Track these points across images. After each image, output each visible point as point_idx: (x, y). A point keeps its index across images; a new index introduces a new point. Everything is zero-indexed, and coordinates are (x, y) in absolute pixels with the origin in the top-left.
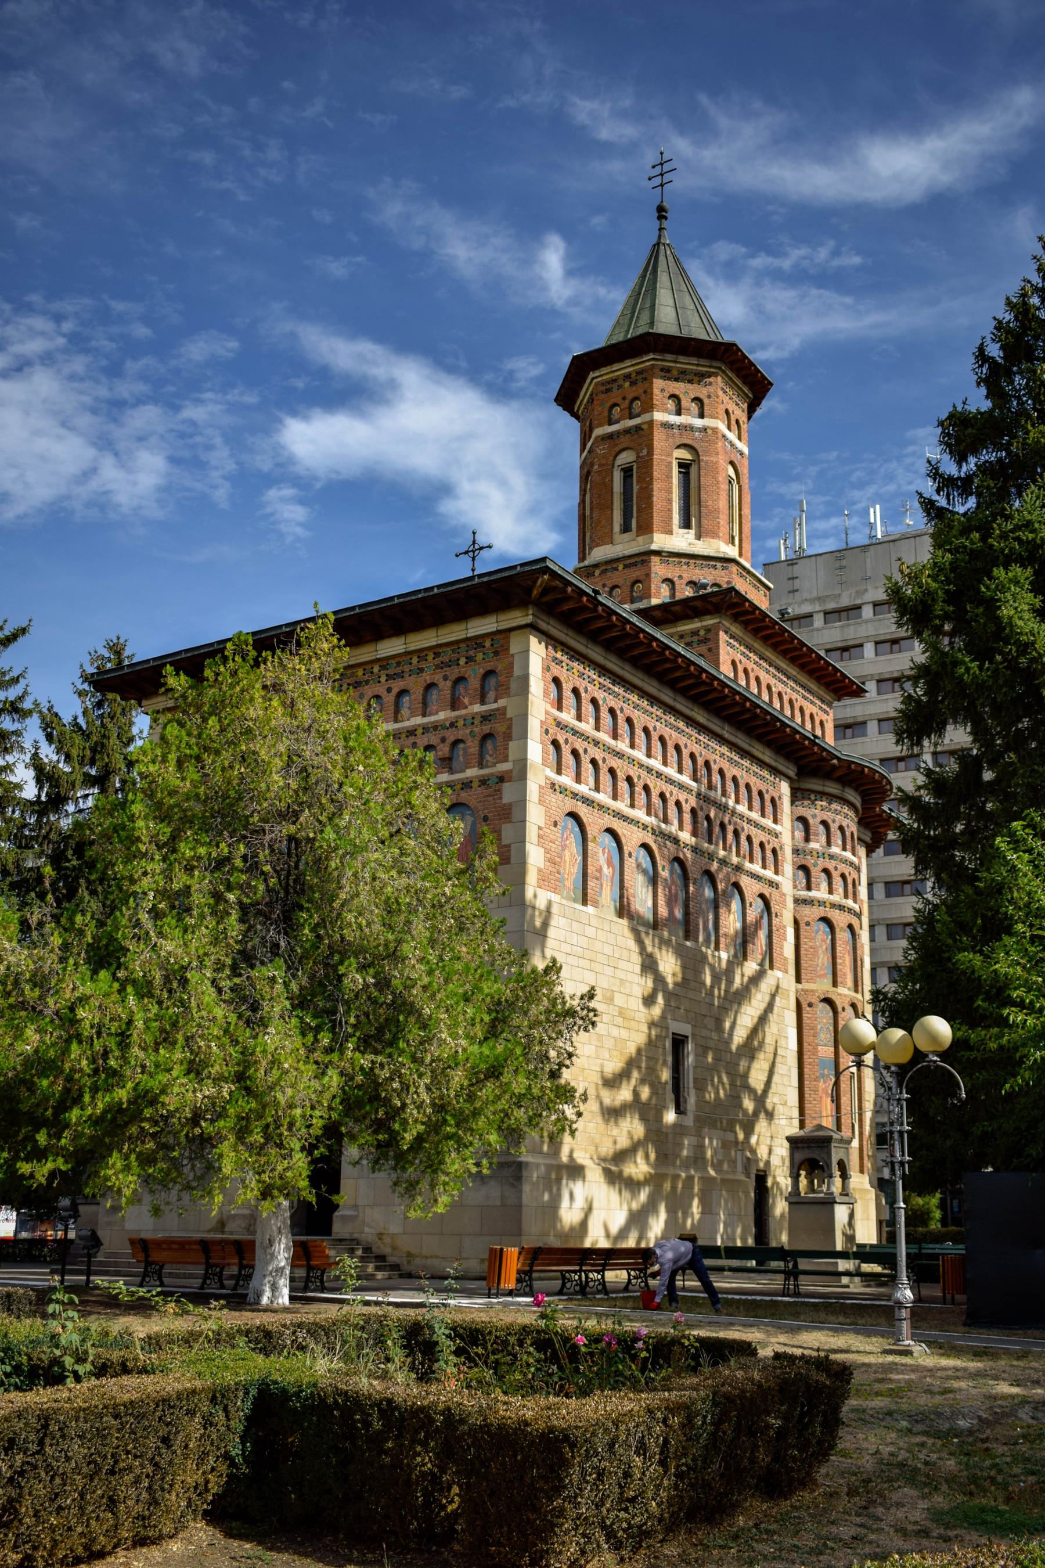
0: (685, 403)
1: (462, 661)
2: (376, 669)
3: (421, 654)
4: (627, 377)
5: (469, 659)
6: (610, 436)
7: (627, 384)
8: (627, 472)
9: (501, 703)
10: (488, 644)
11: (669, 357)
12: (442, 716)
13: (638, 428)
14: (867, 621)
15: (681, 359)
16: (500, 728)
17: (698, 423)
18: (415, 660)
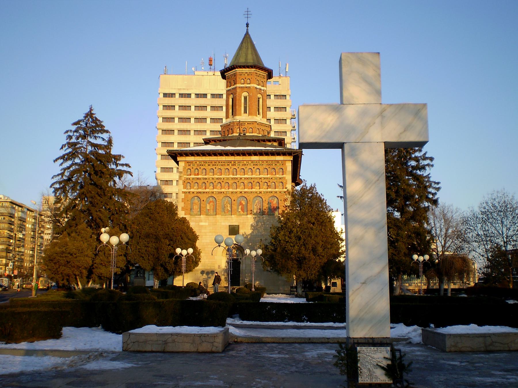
0: (260, 82)
1: (274, 165)
2: (250, 162)
3: (263, 161)
4: (246, 73)
5: (276, 165)
6: (242, 87)
7: (246, 75)
8: (245, 98)
9: (284, 176)
10: (280, 162)
11: (258, 70)
12: (269, 176)
13: (249, 87)
14: (193, 99)
15: (260, 71)
16: (284, 182)
17: (262, 88)
18: (261, 162)
